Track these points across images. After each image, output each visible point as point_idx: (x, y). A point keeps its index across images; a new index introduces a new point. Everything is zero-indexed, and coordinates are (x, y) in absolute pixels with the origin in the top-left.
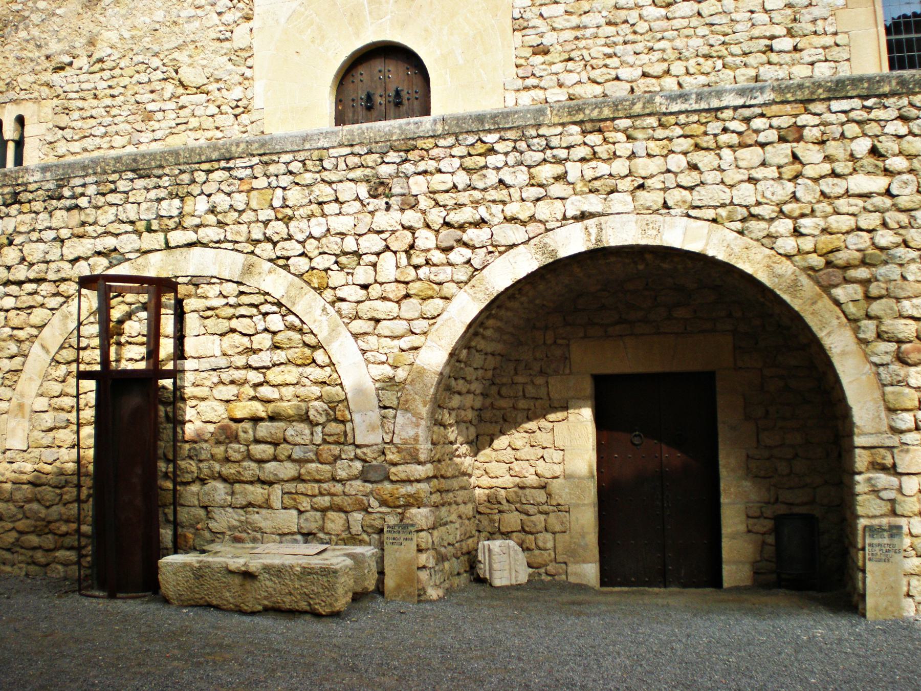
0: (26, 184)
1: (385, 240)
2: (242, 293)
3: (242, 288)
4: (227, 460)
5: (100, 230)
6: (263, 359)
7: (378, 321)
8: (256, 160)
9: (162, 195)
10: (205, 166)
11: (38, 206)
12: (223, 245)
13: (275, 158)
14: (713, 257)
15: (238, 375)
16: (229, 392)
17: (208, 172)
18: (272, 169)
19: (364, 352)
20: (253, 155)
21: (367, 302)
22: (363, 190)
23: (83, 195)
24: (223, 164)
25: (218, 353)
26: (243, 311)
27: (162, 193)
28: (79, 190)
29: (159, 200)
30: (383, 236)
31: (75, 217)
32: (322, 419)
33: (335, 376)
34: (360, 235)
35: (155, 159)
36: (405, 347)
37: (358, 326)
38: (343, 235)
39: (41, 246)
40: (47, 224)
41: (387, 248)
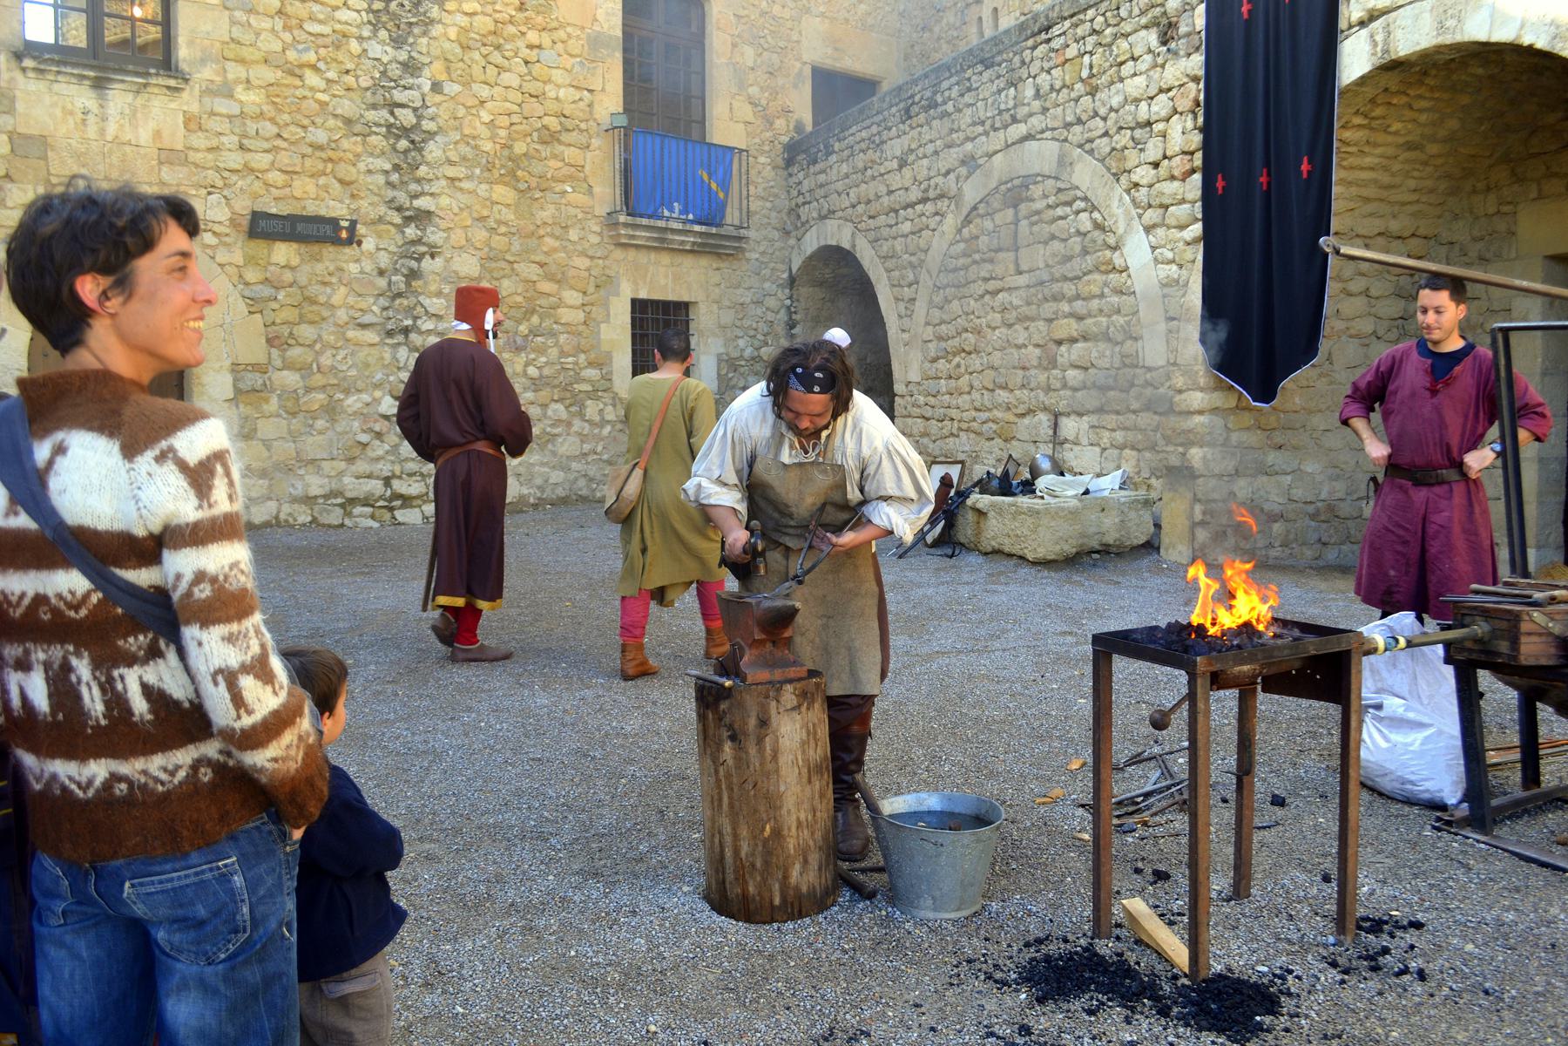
0: (912, 96)
1: (1172, 100)
2: (1060, 190)
3: (1060, 185)
4: (1048, 389)
5: (961, 135)
6: (1077, 266)
7: (1167, 207)
8: (1067, 24)
9: (1002, 85)
10: (1030, 43)
11: (922, 118)
12: (1044, 136)
13: (1081, 16)
14: (1530, 47)
15: (1056, 287)
16: (1048, 309)
17: (1034, 48)
18: (1080, 31)
19: (1153, 248)
20: (1066, 19)
21: (1157, 185)
22: (1152, 37)
23: (950, 99)
24: (1043, 36)
25: (1041, 265)
26: (1060, 211)
27: (1001, 83)
28: (947, 94)
29: (999, 92)
30: (1171, 94)
31: (947, 122)
32: (1119, 338)
33: (1129, 283)
34: (1152, 98)
35: (996, 45)
36: (1188, 239)
37: (1152, 216)
38: (1137, 101)
39: (925, 162)
40: (928, 137)
41: (1175, 112)
